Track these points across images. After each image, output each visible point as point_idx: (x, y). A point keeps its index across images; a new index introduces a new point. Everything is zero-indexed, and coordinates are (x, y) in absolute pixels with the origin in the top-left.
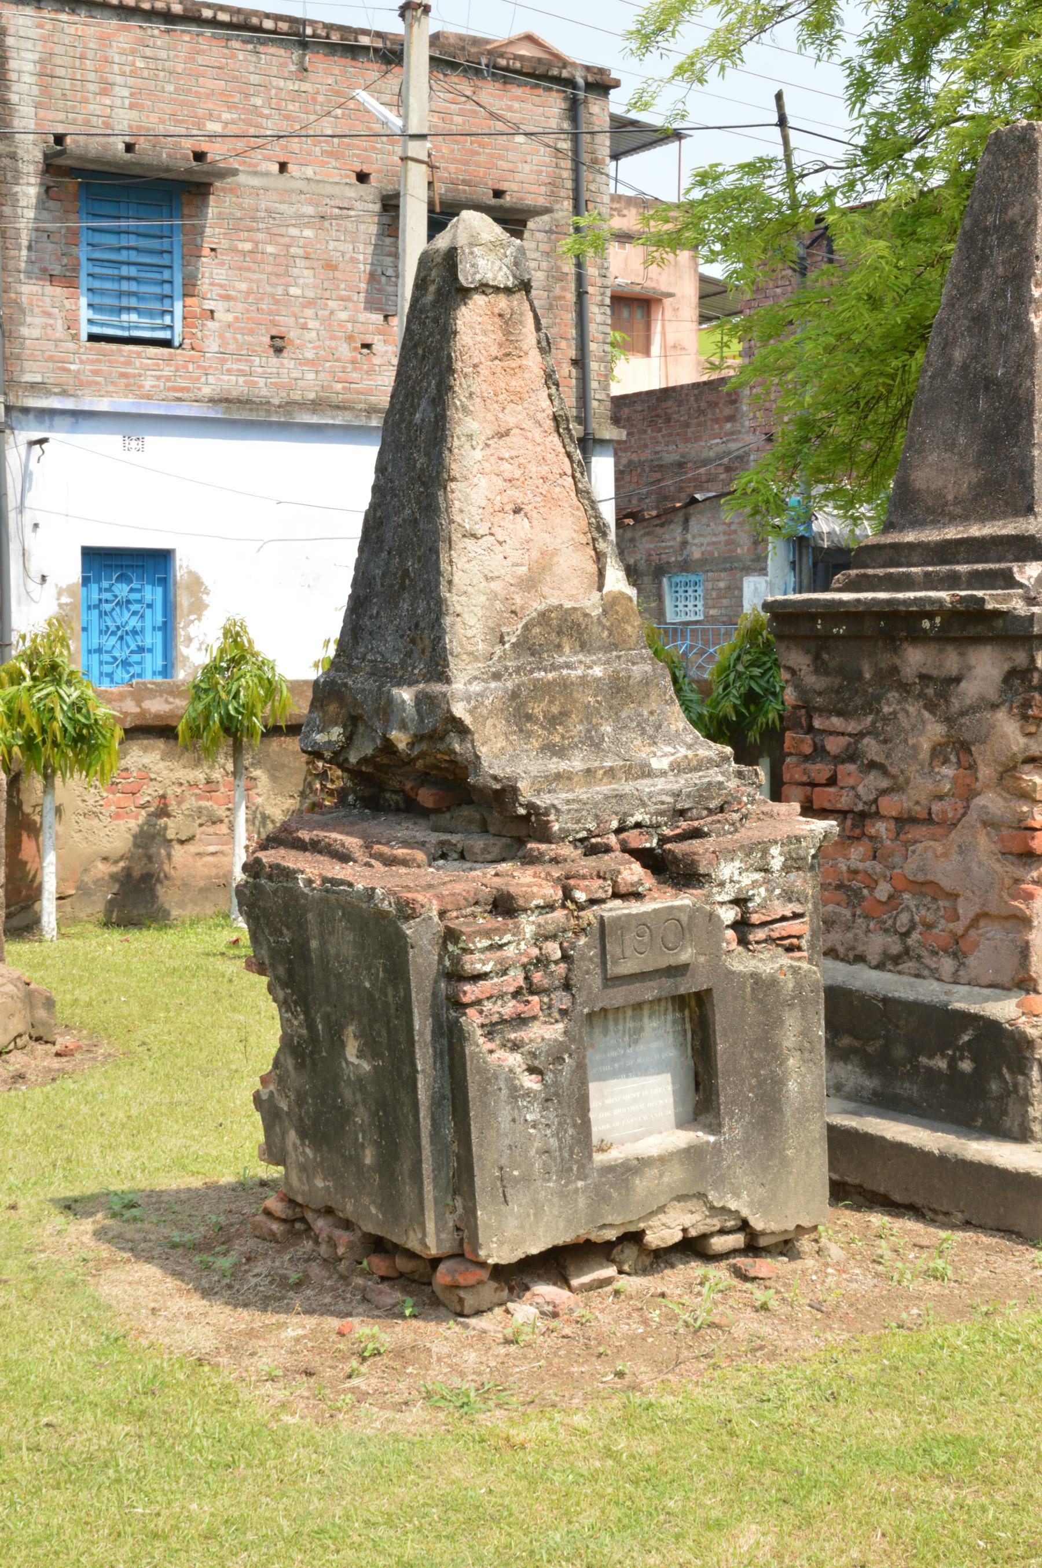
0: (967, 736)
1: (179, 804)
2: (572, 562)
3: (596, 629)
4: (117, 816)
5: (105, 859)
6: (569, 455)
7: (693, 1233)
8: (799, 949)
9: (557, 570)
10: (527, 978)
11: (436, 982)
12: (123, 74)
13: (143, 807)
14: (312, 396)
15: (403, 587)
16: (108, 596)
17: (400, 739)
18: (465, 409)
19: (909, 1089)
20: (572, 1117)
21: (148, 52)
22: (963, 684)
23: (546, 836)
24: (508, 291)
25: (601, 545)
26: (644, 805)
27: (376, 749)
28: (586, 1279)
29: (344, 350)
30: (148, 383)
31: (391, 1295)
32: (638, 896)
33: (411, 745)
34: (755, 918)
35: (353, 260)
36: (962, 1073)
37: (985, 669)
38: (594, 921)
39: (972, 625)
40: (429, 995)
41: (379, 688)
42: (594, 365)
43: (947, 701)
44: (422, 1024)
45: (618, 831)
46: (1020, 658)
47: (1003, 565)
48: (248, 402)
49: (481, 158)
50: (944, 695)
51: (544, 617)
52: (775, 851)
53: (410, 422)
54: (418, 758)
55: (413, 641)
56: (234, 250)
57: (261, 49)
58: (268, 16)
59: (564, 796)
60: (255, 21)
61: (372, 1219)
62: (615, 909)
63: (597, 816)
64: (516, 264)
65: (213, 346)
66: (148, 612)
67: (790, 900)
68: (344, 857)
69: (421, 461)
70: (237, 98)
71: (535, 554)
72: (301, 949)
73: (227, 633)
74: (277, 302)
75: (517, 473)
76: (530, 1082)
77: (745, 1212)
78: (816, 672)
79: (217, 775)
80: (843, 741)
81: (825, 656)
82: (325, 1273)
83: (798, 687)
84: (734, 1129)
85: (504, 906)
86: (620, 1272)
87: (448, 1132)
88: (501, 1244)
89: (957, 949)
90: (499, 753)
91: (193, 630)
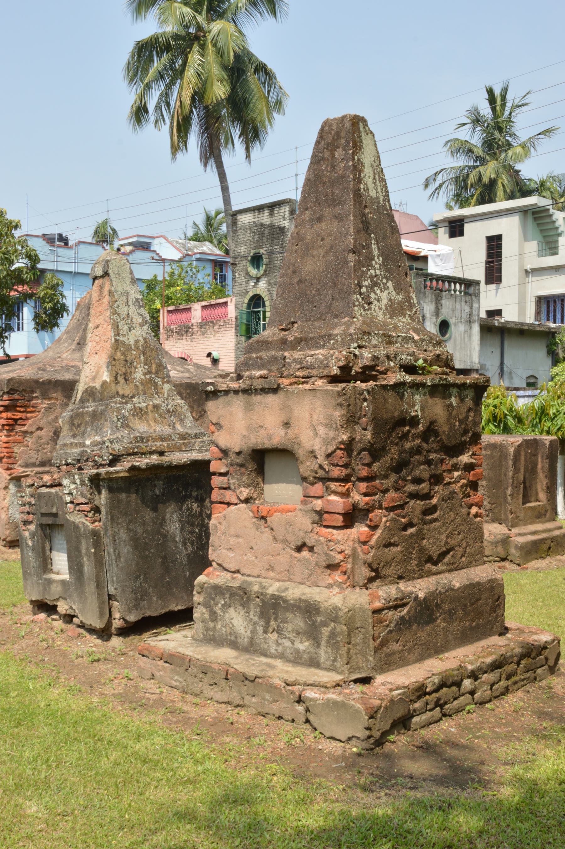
3: (98, 394)
24: (102, 277)
62: (44, 490)
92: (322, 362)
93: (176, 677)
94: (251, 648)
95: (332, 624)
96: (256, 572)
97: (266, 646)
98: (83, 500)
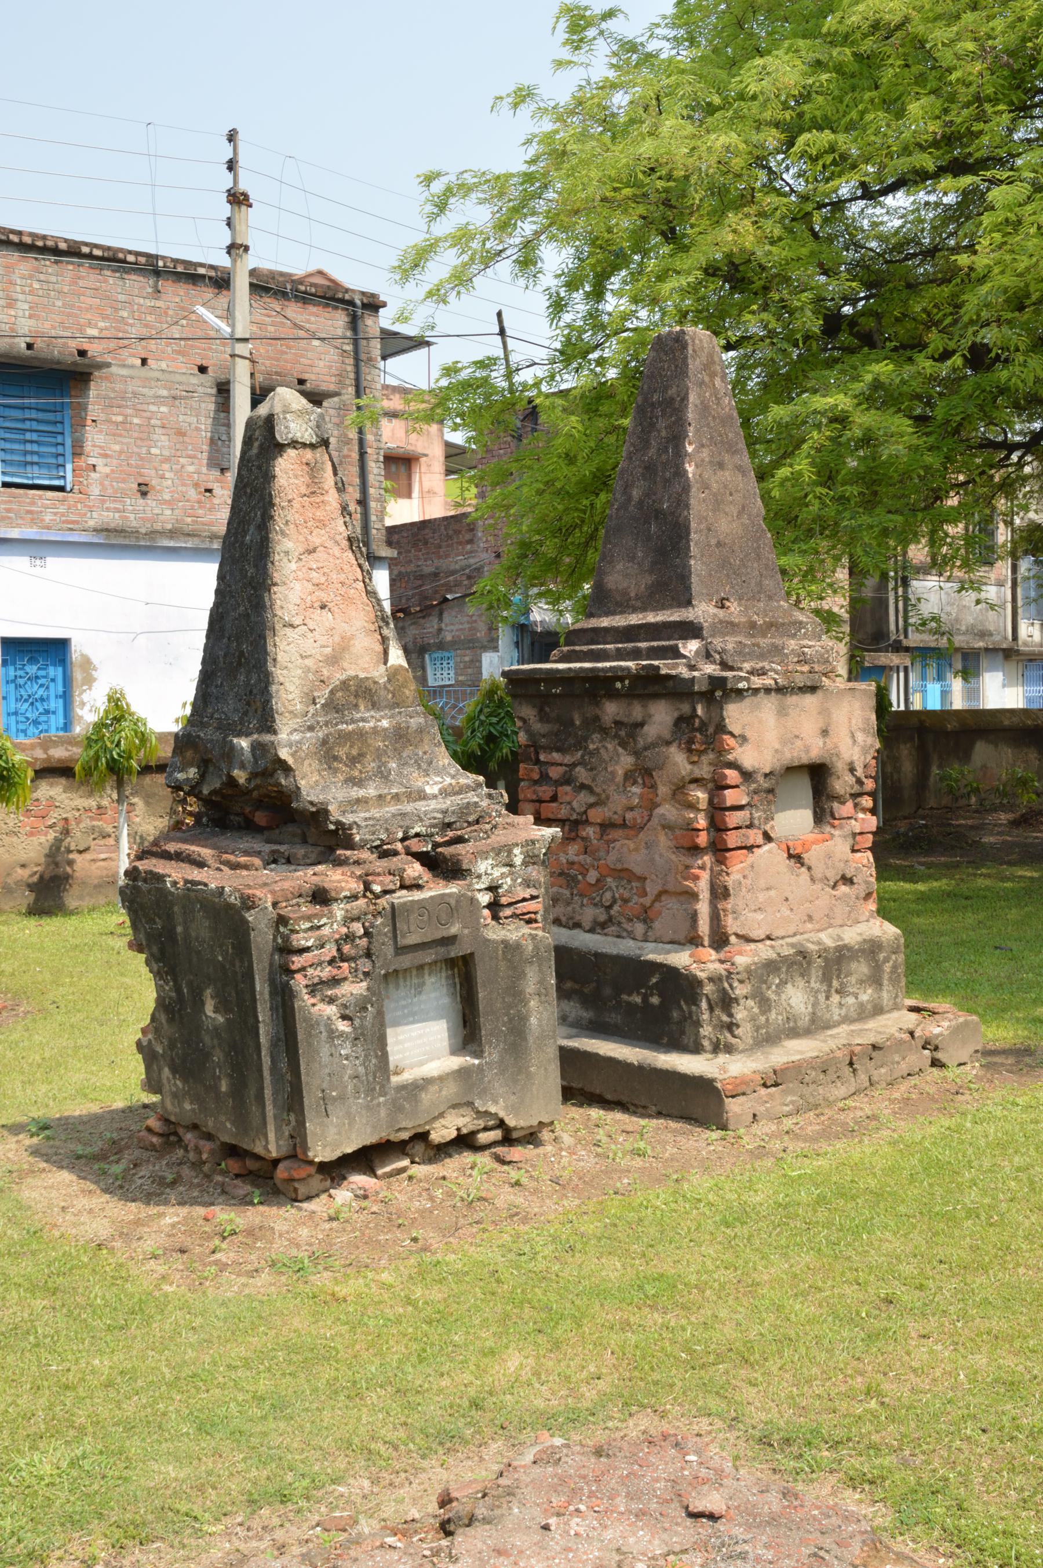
0: (649, 764)
1: (78, 824)
2: (365, 644)
3: (383, 693)
4: (31, 834)
5: (23, 866)
6: (360, 566)
7: (465, 1131)
8: (536, 921)
9: (354, 650)
10: (339, 950)
11: (272, 955)
12: (23, 293)
13: (50, 827)
14: (169, 526)
15: (240, 664)
16: (20, 673)
17: (241, 776)
18: (283, 533)
19: (615, 1018)
20: (375, 1051)
21: (42, 277)
22: (646, 728)
23: (350, 845)
24: (312, 446)
25: (385, 632)
26: (421, 820)
27: (223, 784)
28: (388, 1169)
29: (192, 494)
30: (48, 518)
31: (243, 1188)
32: (419, 887)
33: (248, 780)
34: (504, 900)
35: (197, 429)
36: (652, 1006)
37: (661, 716)
38: (387, 906)
39: (651, 686)
40: (267, 965)
41: (224, 739)
42: (373, 504)
43: (635, 741)
44: (261, 987)
45: (403, 840)
46: (685, 708)
47: (672, 643)
48: (122, 531)
49: (289, 357)
50: (632, 736)
51: (345, 684)
52: (517, 851)
53: (242, 542)
54: (254, 789)
56: (109, 421)
57: (126, 276)
58: (130, 252)
59: (362, 815)
60: (121, 256)
61: (228, 1132)
62: (403, 897)
63: (387, 829)
64: (318, 427)
65: (95, 491)
66: (52, 685)
67: (528, 887)
68: (201, 864)
69: (251, 571)
70: (109, 311)
71: (337, 639)
72: (169, 933)
73: (110, 699)
74: (142, 459)
75: (323, 580)
76: (343, 1026)
77: (502, 1114)
78: (541, 720)
79: (105, 802)
80: (561, 770)
81: (547, 709)
82: (193, 1174)
83: (529, 732)
84: (493, 1054)
85: (321, 897)
86: (412, 1162)
87: (283, 1065)
88: (324, 1146)
89: (646, 916)
90: (314, 785)
91: (85, 697)
92: (822, 656)
93: (789, 1099)
94: (816, 1025)
95: (893, 957)
96: (792, 930)
97: (828, 1016)
98: (527, 893)
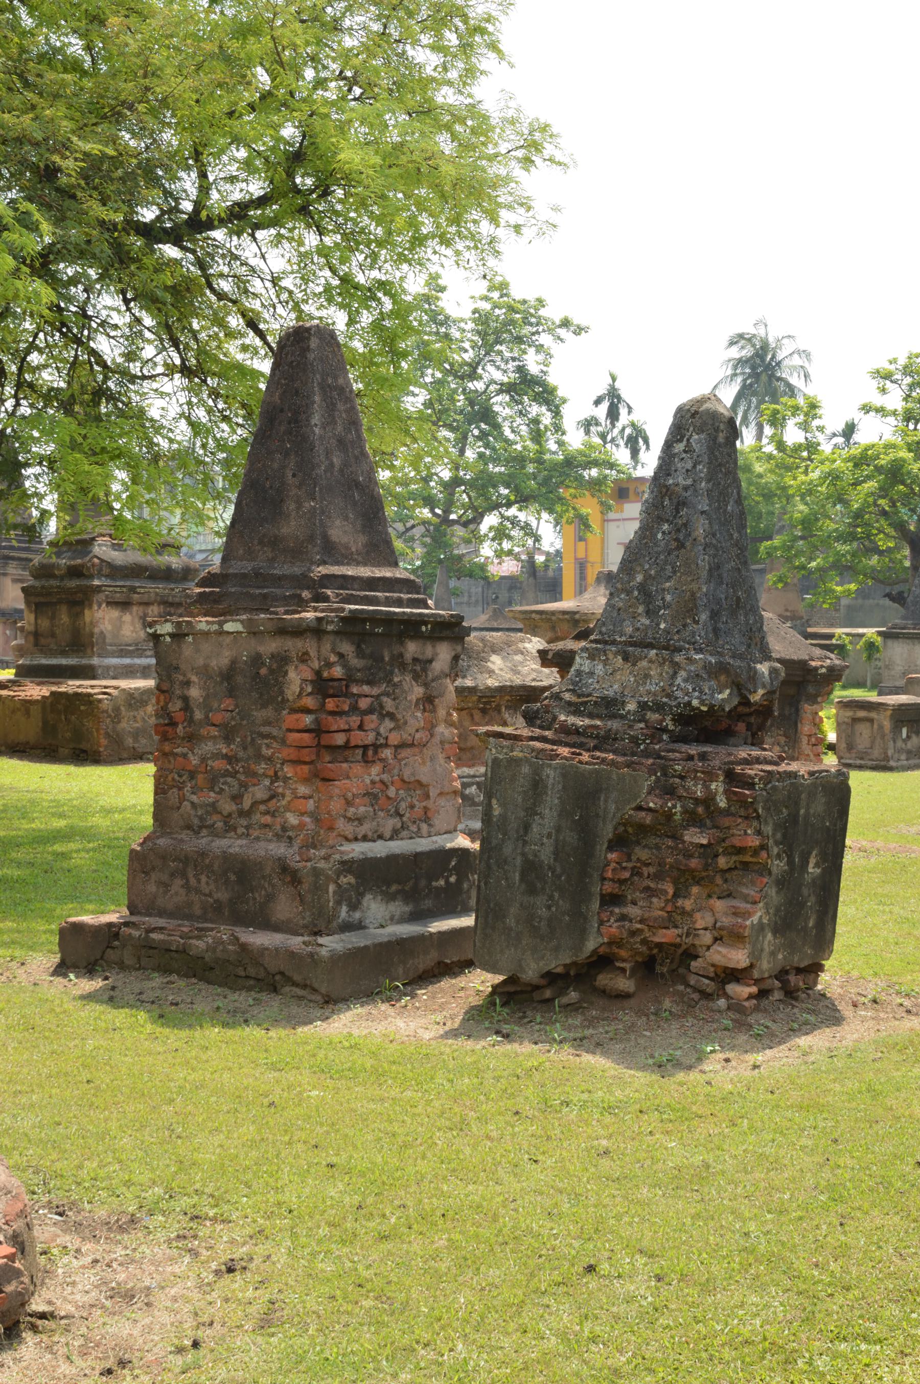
0: (435, 694)
19: (428, 903)
50: (425, 670)
53: (725, 511)
55: (750, 638)
78: (358, 657)
80: (369, 700)
83: (345, 666)
89: (426, 818)
